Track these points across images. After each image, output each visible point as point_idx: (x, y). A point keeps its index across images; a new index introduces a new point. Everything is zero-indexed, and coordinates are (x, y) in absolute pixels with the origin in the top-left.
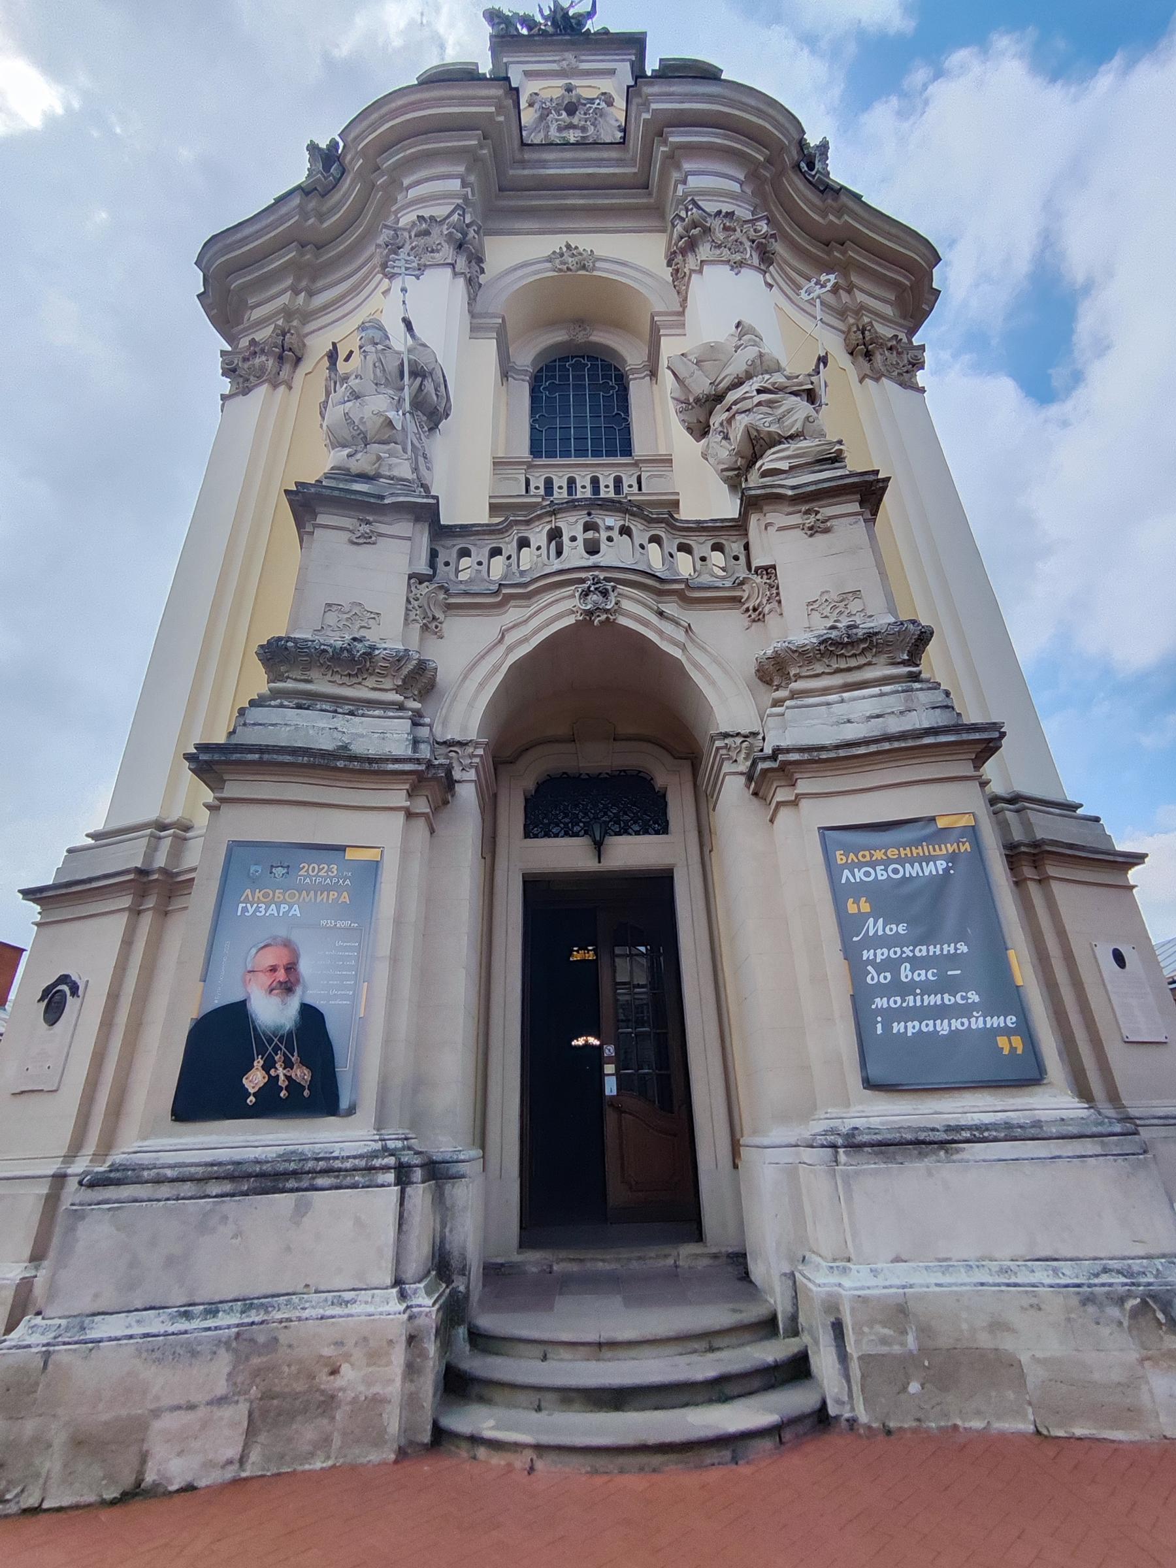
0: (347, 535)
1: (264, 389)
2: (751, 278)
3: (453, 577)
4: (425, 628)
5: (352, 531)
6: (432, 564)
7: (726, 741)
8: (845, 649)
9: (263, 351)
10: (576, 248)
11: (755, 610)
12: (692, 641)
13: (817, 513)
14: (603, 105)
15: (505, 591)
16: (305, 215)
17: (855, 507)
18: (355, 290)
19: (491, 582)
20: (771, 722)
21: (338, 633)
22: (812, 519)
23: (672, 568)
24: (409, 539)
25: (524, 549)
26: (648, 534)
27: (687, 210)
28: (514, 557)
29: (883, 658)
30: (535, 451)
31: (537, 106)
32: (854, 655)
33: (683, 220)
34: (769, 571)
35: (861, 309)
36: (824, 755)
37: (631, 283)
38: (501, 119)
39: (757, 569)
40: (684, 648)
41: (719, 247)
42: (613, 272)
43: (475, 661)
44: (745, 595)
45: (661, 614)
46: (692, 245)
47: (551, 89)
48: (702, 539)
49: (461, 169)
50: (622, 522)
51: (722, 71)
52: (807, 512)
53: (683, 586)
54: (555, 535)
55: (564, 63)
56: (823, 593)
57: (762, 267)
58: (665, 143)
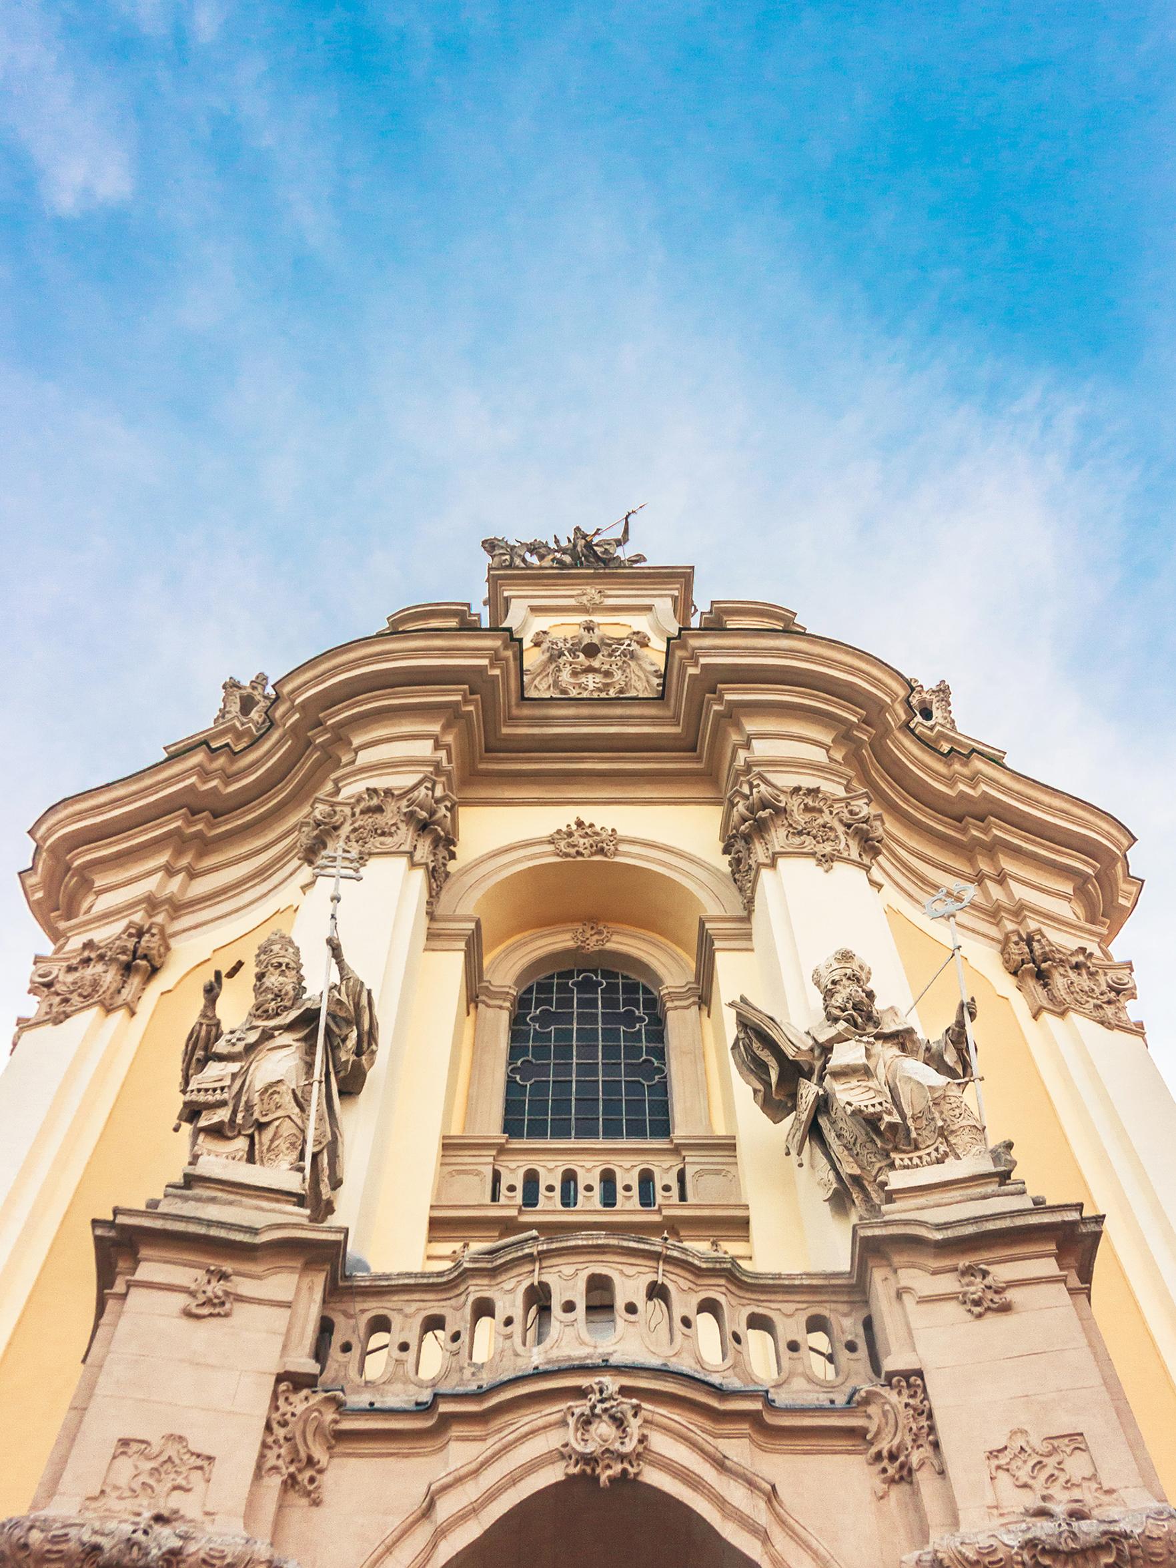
2: (847, 876)
3: (353, 1372)
4: (291, 1483)
5: (193, 1294)
6: (320, 1353)
10: (591, 826)
12: (782, 1522)
13: (985, 1274)
14: (635, 646)
15: (444, 1408)
17: (1048, 1267)
18: (261, 874)
19: (421, 1385)
22: (976, 1287)
23: (739, 1366)
24: (287, 1305)
25: (485, 1321)
26: (695, 1300)
27: (751, 787)
28: (465, 1337)
30: (511, 1127)
31: (545, 646)
33: (746, 797)
34: (912, 1379)
39: (890, 1375)
40: (765, 1537)
41: (800, 833)
44: (873, 1429)
45: (720, 1464)
47: (565, 628)
48: (789, 1308)
50: (651, 1277)
52: (969, 1271)
53: (757, 1406)
54: (539, 1298)
55: (584, 600)
56: (1014, 1433)
57: (866, 860)
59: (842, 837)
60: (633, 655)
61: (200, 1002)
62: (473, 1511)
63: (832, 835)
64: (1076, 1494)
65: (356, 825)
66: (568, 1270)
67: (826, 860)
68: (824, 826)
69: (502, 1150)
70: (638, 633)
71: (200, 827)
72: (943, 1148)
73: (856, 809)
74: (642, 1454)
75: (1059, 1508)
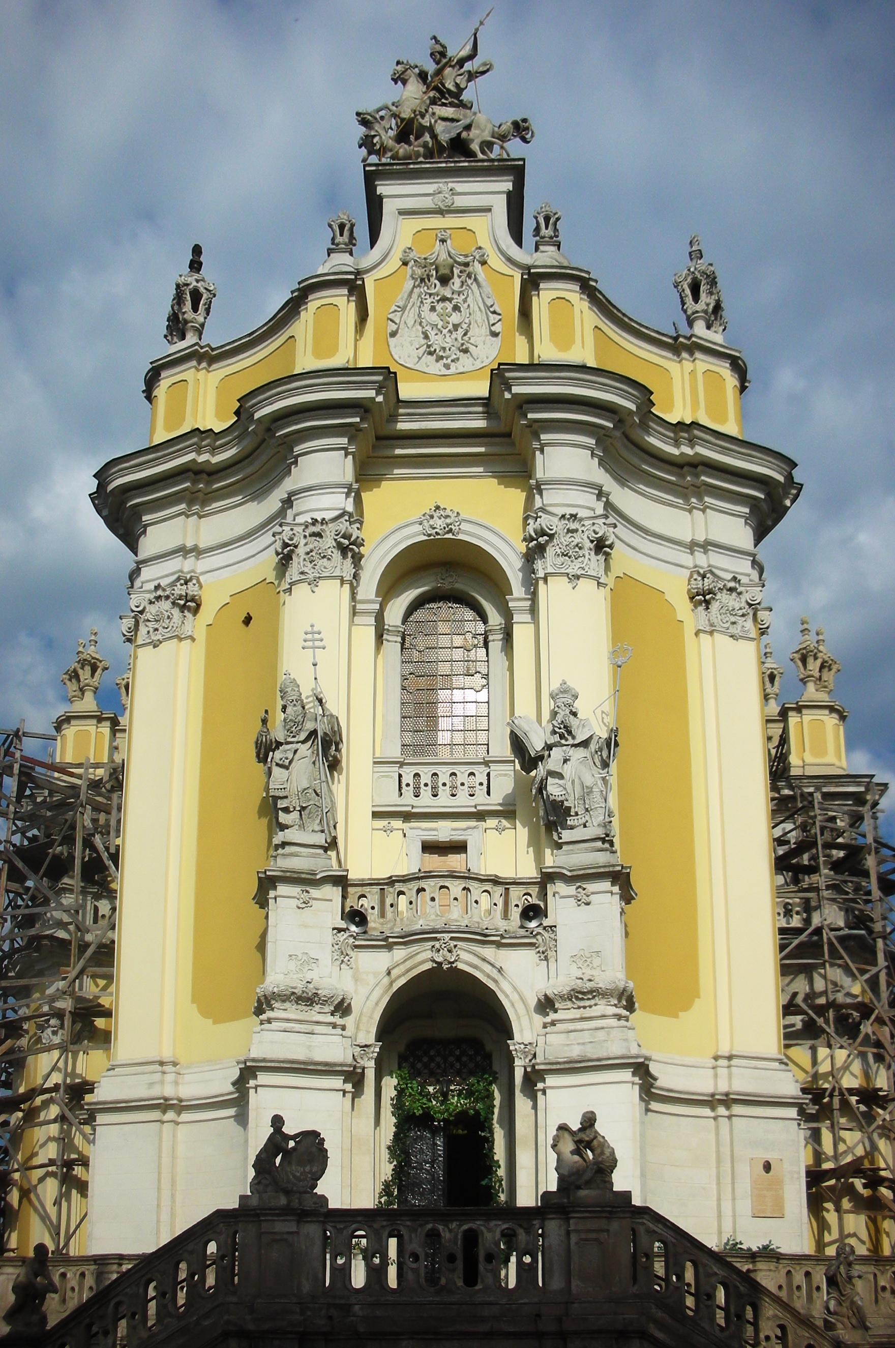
0: (294, 903)
15: (391, 940)
21: (295, 976)
29: (603, 1002)
32: (589, 999)
41: (563, 555)
43: (371, 981)
46: (541, 550)
50: (463, 886)
59: (586, 552)
63: (581, 553)
64: (594, 972)
66: (432, 884)
68: (577, 545)
69: (402, 764)
70: (480, 248)
72: (587, 818)
73: (597, 530)
75: (586, 978)
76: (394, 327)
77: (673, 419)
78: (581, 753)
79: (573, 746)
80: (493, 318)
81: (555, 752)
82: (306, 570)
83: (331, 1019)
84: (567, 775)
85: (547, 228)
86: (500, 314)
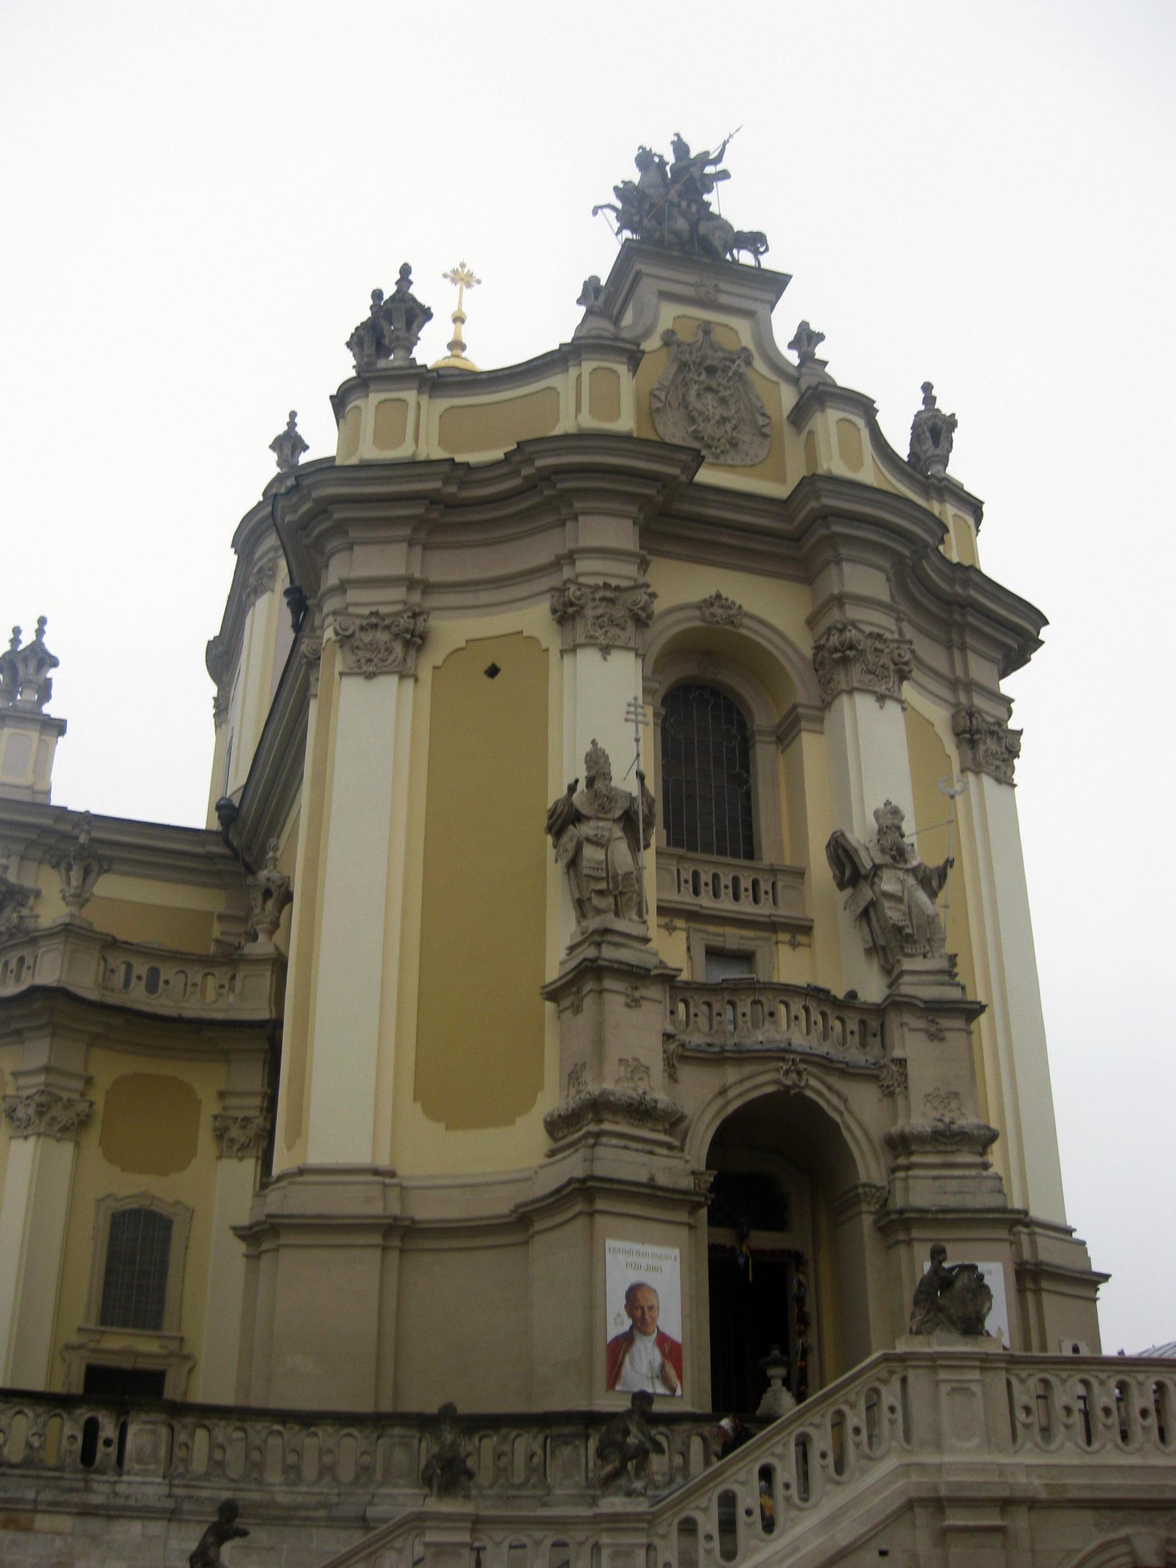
0: (621, 999)
1: (395, 679)
2: (892, 708)
5: (628, 996)
7: (867, 1189)
8: (947, 1138)
9: (387, 627)
11: (888, 1087)
12: (847, 1108)
15: (727, 1054)
16: (447, 481)
20: (898, 1184)
31: (674, 349)
32: (951, 1144)
34: (902, 1062)
35: (970, 686)
36: (930, 1216)
37: (775, 651)
38: (683, 478)
40: (841, 1114)
41: (870, 672)
42: (755, 632)
46: (845, 661)
49: (634, 509)
51: (874, 402)
52: (932, 1021)
53: (844, 1066)
58: (828, 527)
59: (892, 674)
60: (740, 376)
61: (565, 791)
62: (740, 1095)
65: (600, 611)
67: (881, 698)
68: (883, 666)
70: (745, 349)
71: (434, 515)
73: (903, 653)
74: (807, 1086)
75: (947, 1120)
76: (660, 405)
77: (955, 560)
78: (911, 881)
79: (907, 871)
80: (761, 421)
81: (886, 874)
82: (597, 635)
83: (667, 1138)
84: (906, 898)
85: (809, 345)
86: (768, 417)
